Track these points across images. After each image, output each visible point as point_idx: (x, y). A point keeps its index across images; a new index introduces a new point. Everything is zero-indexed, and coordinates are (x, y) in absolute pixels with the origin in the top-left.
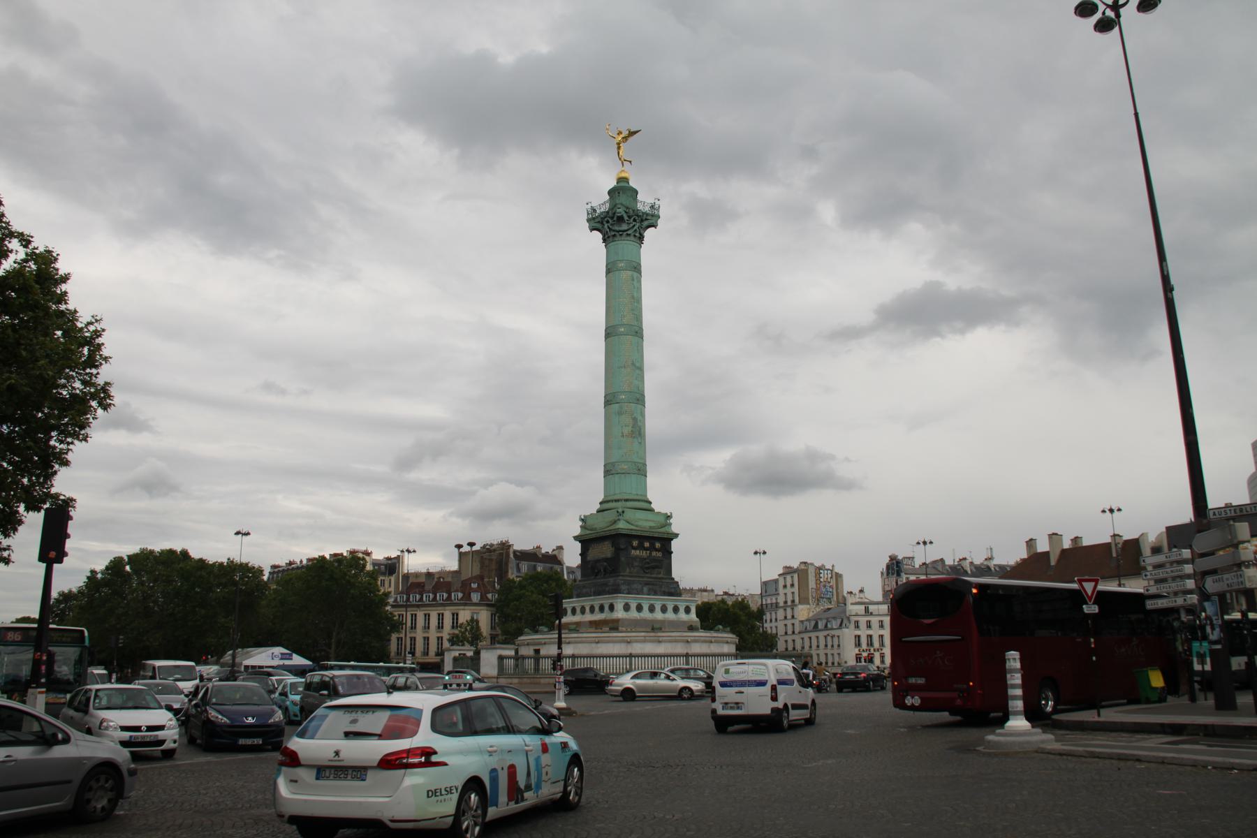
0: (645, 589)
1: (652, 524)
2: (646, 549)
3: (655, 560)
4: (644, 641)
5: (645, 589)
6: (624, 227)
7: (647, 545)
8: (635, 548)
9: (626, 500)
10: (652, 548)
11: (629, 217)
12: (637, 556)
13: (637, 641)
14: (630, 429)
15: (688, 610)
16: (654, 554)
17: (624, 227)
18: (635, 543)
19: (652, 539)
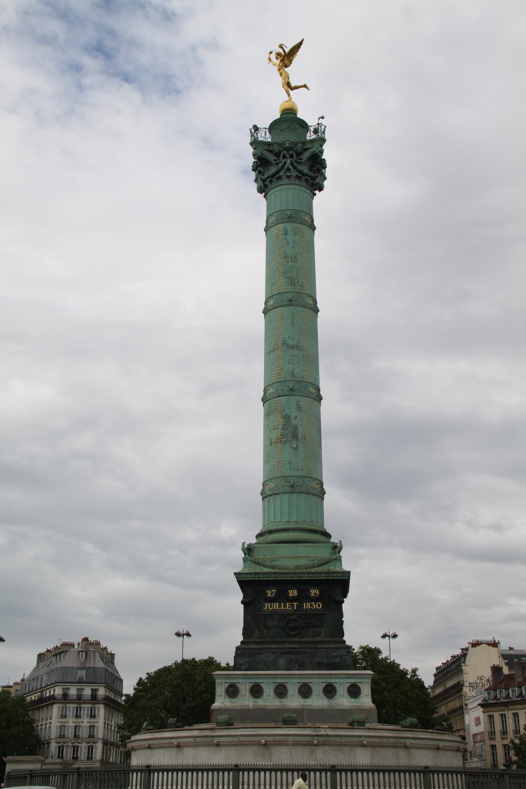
0: (282, 661)
1: (302, 562)
2: (293, 600)
3: (309, 614)
4: (196, 745)
5: (282, 661)
6: (273, 170)
7: (293, 593)
8: (271, 601)
9: (270, 532)
10: (300, 599)
11: (277, 155)
12: (274, 613)
13: (187, 745)
14: (278, 432)
15: (354, 691)
16: (307, 606)
17: (273, 170)
18: (270, 593)
19: (303, 584)
